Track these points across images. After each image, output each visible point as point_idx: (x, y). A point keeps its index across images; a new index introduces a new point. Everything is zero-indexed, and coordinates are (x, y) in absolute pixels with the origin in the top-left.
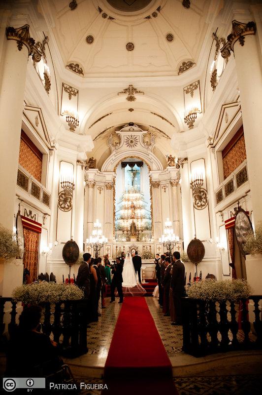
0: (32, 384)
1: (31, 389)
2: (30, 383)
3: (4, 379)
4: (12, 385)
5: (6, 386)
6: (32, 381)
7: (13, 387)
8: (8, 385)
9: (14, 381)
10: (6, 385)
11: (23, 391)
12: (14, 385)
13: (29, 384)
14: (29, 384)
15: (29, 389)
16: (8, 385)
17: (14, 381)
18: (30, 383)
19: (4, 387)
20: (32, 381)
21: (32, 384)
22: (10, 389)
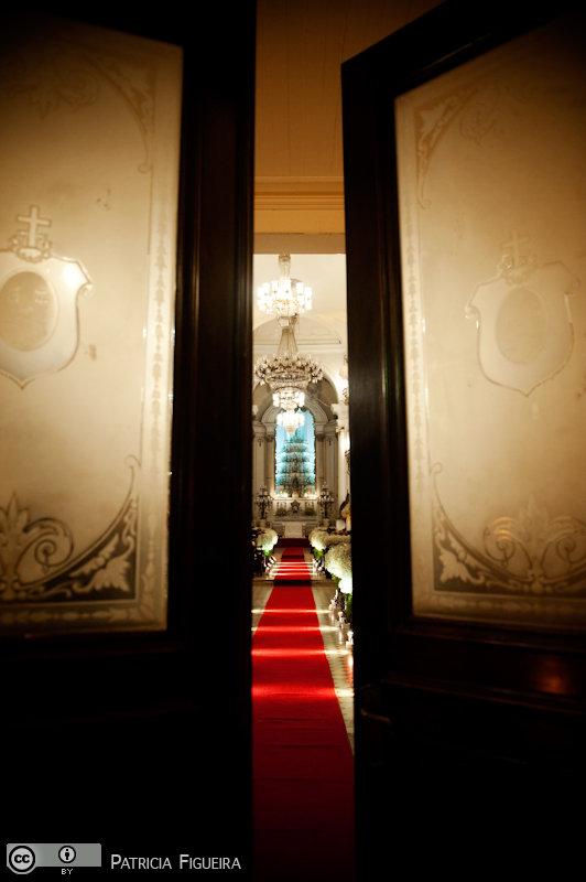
0: (71, 858)
1: (70, 868)
2: (67, 855)
3: (10, 847)
4: (26, 859)
5: (14, 862)
6: (71, 851)
7: (30, 864)
8: (19, 859)
9: (30, 850)
10: (13, 859)
11: (52, 872)
12: (31, 859)
13: (64, 858)
14: (64, 858)
15: (66, 868)
16: (19, 859)
17: (30, 850)
18: (67, 855)
19: (8, 865)
20: (71, 851)
21: (71, 858)
22: (22, 868)
